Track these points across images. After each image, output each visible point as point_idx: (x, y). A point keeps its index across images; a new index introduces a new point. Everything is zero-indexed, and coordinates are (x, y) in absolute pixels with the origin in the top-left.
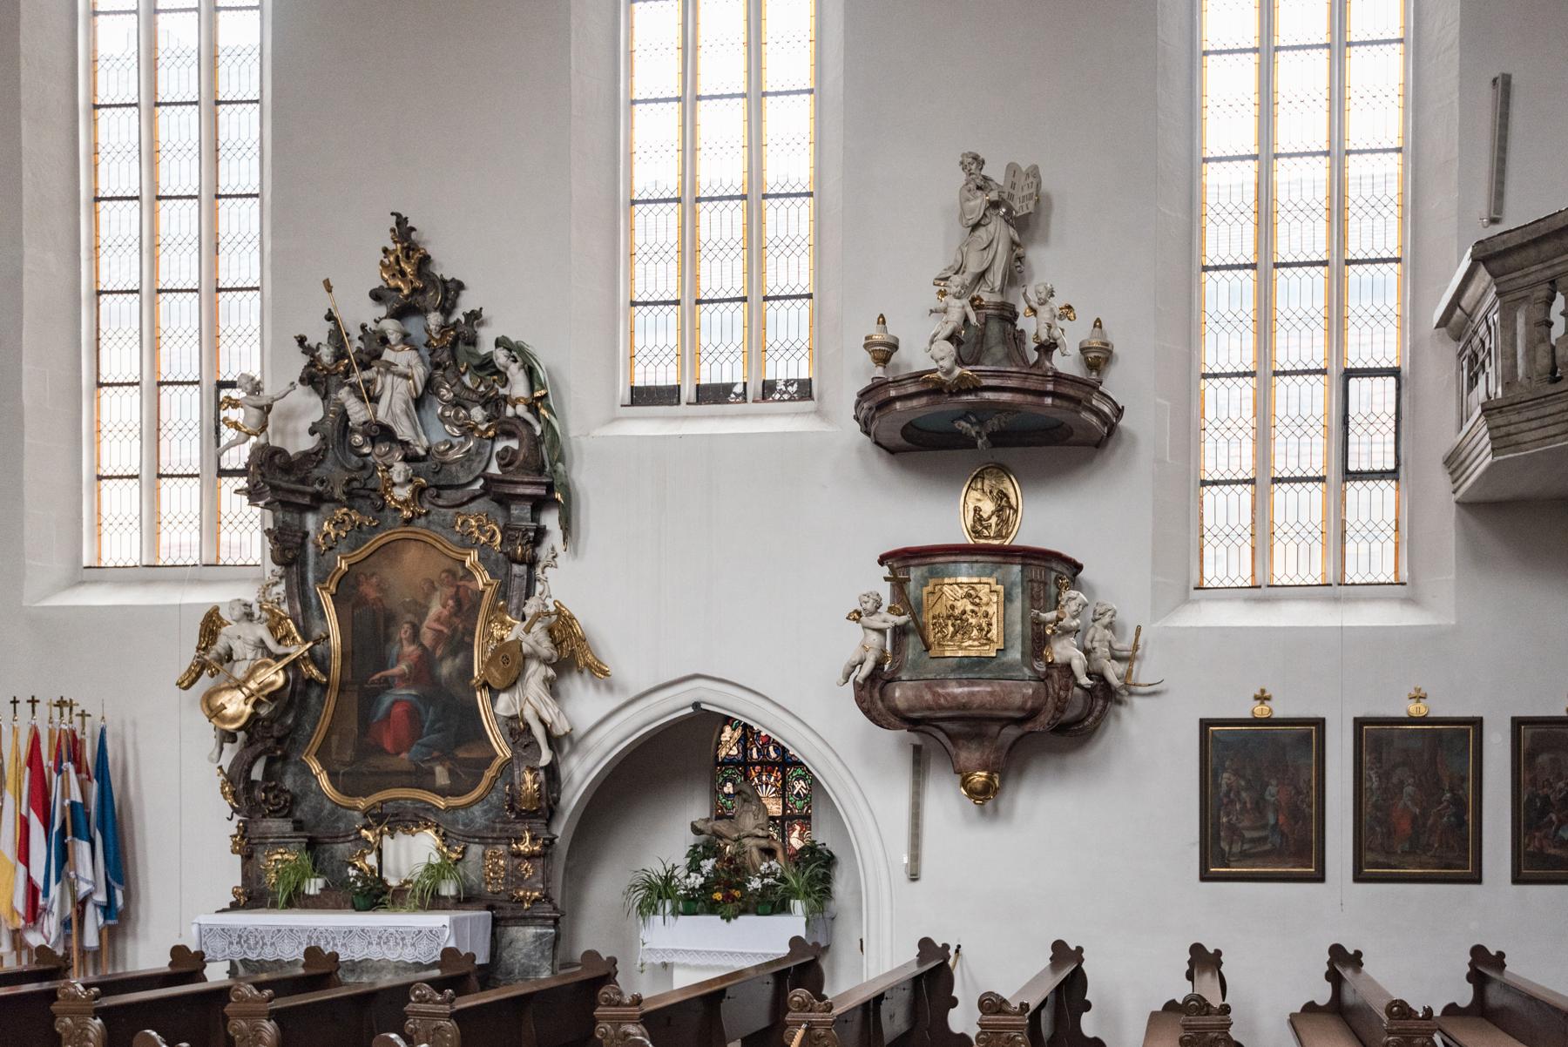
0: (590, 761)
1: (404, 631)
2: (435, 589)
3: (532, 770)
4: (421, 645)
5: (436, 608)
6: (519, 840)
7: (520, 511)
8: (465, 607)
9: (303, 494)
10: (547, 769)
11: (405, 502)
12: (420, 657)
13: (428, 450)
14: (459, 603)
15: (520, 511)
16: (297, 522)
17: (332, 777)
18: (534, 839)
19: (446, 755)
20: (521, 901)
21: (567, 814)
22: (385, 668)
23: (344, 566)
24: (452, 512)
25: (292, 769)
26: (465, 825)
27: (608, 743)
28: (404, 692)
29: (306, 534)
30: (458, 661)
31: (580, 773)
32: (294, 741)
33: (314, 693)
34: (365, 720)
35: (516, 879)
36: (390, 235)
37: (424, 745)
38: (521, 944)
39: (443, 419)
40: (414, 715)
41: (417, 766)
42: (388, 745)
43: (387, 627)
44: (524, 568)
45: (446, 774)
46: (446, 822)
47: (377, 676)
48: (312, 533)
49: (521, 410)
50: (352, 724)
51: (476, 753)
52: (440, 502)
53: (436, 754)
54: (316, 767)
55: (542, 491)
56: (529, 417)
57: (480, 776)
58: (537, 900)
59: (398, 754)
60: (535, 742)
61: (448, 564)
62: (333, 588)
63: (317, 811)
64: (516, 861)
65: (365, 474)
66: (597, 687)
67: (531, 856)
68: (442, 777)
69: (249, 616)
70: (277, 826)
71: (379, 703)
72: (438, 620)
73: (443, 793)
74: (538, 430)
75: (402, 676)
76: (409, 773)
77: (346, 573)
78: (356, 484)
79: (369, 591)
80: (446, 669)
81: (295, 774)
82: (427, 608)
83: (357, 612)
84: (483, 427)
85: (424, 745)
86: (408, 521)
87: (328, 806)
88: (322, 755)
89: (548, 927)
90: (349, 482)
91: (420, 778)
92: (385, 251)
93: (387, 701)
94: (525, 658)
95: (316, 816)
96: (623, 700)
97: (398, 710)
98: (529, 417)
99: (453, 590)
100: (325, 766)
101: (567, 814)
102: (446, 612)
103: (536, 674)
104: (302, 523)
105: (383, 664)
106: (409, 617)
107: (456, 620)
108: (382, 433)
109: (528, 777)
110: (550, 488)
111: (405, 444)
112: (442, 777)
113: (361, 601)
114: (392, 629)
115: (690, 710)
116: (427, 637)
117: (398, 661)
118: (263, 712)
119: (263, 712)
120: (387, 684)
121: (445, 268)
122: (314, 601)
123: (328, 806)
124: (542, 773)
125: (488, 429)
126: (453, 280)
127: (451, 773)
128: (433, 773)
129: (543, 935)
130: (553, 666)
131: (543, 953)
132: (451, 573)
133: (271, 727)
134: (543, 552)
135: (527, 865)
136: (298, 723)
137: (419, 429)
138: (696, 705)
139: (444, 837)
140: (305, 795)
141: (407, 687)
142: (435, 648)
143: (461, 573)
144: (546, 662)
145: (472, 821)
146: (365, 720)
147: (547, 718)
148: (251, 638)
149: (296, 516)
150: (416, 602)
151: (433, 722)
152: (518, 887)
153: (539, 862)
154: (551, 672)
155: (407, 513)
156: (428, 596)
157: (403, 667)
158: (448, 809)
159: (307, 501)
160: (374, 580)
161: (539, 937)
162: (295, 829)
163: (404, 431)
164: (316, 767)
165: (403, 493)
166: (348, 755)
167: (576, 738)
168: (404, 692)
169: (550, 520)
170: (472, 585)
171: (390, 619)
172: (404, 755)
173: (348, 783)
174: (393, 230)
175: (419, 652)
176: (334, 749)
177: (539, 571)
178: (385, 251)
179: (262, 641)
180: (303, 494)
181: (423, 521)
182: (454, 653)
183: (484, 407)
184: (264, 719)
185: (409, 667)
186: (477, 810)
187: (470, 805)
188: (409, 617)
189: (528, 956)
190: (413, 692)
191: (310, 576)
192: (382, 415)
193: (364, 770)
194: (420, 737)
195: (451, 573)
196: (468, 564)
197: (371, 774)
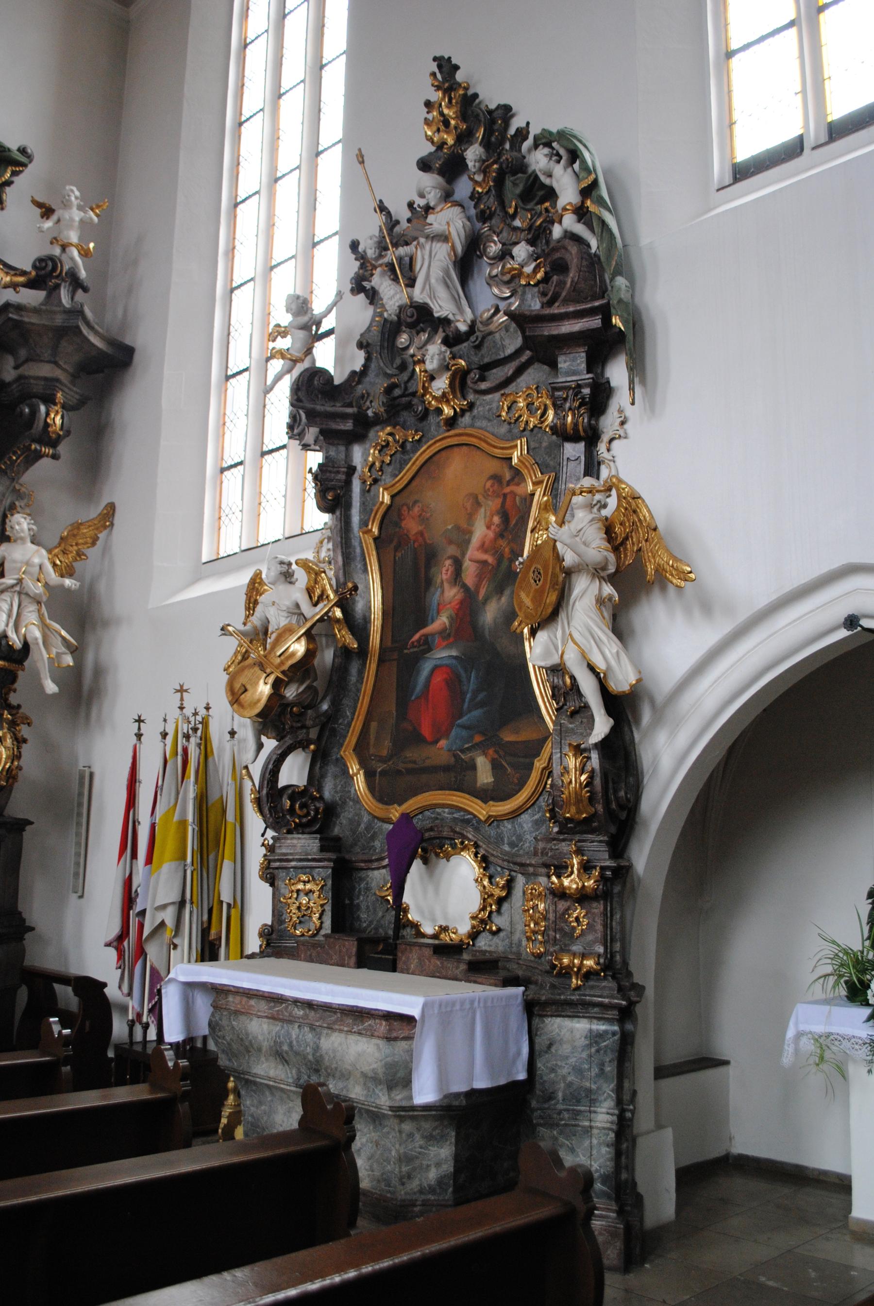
0: (683, 737)
1: (444, 571)
2: (478, 504)
3: (578, 750)
4: (464, 586)
5: (480, 532)
6: (561, 869)
7: (573, 366)
8: (512, 522)
9: (344, 417)
10: (605, 746)
11: (444, 398)
12: (461, 602)
13: (472, 326)
14: (505, 517)
15: (573, 366)
16: (342, 456)
17: (369, 776)
18: (586, 868)
19: (489, 739)
20: (565, 973)
21: (654, 827)
22: (425, 625)
23: (387, 499)
24: (497, 396)
25: (332, 769)
26: (512, 845)
27: (710, 704)
28: (444, 654)
29: (352, 470)
30: (503, 599)
31: (671, 757)
32: (333, 731)
33: (354, 669)
34: (403, 702)
35: (559, 934)
36: (429, 81)
37: (463, 727)
38: (566, 1049)
39: (492, 280)
40: (454, 684)
41: (455, 756)
42: (426, 731)
43: (428, 567)
44: (581, 446)
45: (489, 767)
46: (487, 839)
47: (417, 636)
48: (359, 468)
49: (569, 222)
50: (390, 706)
51: (526, 734)
52: (483, 386)
53: (478, 739)
54: (354, 767)
55: (596, 322)
56: (580, 229)
57: (530, 767)
58: (589, 975)
59: (437, 742)
60: (587, 707)
61: (493, 467)
62: (375, 530)
63: (355, 823)
64: (562, 905)
65: (405, 376)
66: (688, 612)
67: (582, 897)
68: (484, 775)
69: (287, 576)
70: (303, 844)
71: (418, 672)
72: (482, 547)
73: (486, 795)
74: (594, 243)
75: (443, 633)
76: (447, 769)
77: (390, 507)
78: (397, 392)
79: (411, 526)
80: (490, 614)
81: (335, 777)
82: (470, 533)
83: (399, 554)
84: (528, 269)
85: (463, 727)
86: (451, 422)
87: (366, 818)
88: (360, 750)
89: (610, 1021)
90: (389, 390)
91: (458, 775)
92: (428, 104)
93: (426, 668)
94: (569, 573)
95: (354, 831)
96: (725, 628)
97: (438, 679)
98: (580, 229)
99: (499, 501)
100: (363, 764)
101: (654, 827)
102: (491, 534)
103: (585, 593)
104: (348, 456)
105: (422, 621)
106: (452, 550)
107: (503, 543)
108: (421, 317)
109: (572, 762)
110: (606, 312)
111: (445, 322)
112: (484, 775)
113: (402, 541)
114: (433, 570)
115: (844, 633)
116: (470, 571)
117: (438, 613)
118: (291, 693)
119: (291, 693)
120: (427, 645)
121: (491, 97)
122: (358, 550)
123: (366, 818)
124: (595, 756)
125: (535, 271)
126: (499, 107)
127: (496, 766)
128: (473, 767)
129: (601, 1036)
130: (612, 579)
131: (602, 1065)
132: (496, 478)
133: (302, 715)
134: (609, 423)
135: (578, 911)
136: (336, 705)
137: (464, 301)
138: (851, 622)
139: (485, 862)
140: (344, 803)
141: (449, 647)
142: (478, 586)
143: (508, 476)
144: (598, 572)
145: (520, 838)
146: (403, 702)
147: (601, 665)
148: (287, 603)
149: (342, 448)
150: (457, 528)
151: (475, 693)
152: (565, 950)
153: (598, 908)
154: (608, 590)
155: (447, 411)
156: (471, 517)
157: (443, 620)
158: (494, 820)
159: (349, 425)
160: (416, 509)
161: (595, 1038)
162: (323, 849)
163: (442, 307)
164: (354, 767)
165: (441, 384)
166: (387, 745)
167: (659, 699)
168: (444, 654)
169: (617, 373)
170: (519, 490)
171: (431, 556)
172: (443, 743)
173: (385, 789)
174: (433, 74)
175: (459, 597)
176: (372, 741)
177: (602, 447)
178: (428, 104)
179: (297, 606)
180: (344, 417)
181: (467, 419)
182: (499, 590)
183: (532, 242)
184: (292, 704)
185: (451, 618)
186: (526, 820)
187: (515, 815)
188: (452, 550)
189: (578, 1071)
190: (454, 653)
191: (356, 519)
192: (419, 294)
193: (401, 766)
194: (461, 716)
195: (496, 478)
196: (515, 461)
197: (410, 771)
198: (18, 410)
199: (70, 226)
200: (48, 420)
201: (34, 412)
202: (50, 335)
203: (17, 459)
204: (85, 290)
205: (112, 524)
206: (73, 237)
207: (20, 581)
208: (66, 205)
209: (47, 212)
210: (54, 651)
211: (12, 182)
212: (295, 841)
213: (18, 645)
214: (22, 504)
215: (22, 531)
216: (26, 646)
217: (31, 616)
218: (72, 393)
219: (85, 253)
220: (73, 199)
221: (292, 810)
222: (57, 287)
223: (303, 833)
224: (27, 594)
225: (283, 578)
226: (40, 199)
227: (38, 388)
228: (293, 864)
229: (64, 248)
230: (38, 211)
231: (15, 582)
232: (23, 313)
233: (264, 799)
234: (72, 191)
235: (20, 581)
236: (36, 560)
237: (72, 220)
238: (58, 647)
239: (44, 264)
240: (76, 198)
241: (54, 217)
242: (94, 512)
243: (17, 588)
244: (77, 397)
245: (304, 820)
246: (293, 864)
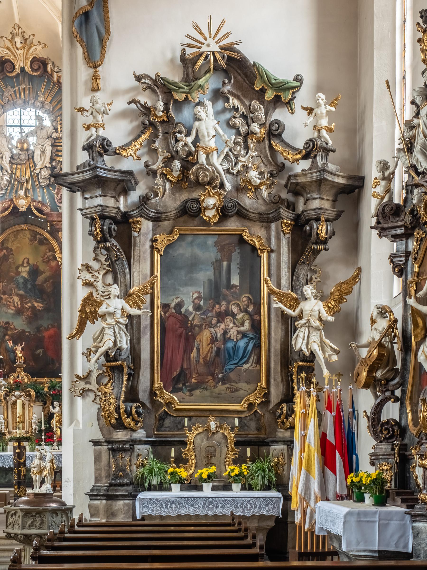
159: (402, 231)
198: (304, 229)
199: (321, 117)
200: (318, 232)
201: (311, 228)
202: (315, 185)
203: (309, 254)
204: (333, 151)
205: (360, 279)
206: (324, 122)
207: (308, 320)
208: (318, 106)
209: (310, 111)
210: (327, 354)
211: (295, 97)
212: (382, 446)
213: (308, 354)
214: (316, 276)
215: (308, 294)
216: (312, 353)
217: (315, 337)
218: (332, 212)
219: (330, 130)
220: (320, 101)
221: (381, 431)
222: (316, 156)
223: (387, 442)
224: (312, 327)
225: (380, 316)
226: (305, 106)
227: (312, 214)
228: (381, 457)
229: (319, 131)
230: (306, 112)
231: (306, 321)
232: (298, 178)
233: (371, 427)
234: (319, 97)
235: (308, 320)
236: (316, 308)
237: (322, 113)
238: (329, 352)
239: (308, 146)
240: (323, 100)
241: (313, 114)
242: (351, 273)
243: (307, 325)
244: (334, 213)
245: (387, 436)
246: (381, 457)
